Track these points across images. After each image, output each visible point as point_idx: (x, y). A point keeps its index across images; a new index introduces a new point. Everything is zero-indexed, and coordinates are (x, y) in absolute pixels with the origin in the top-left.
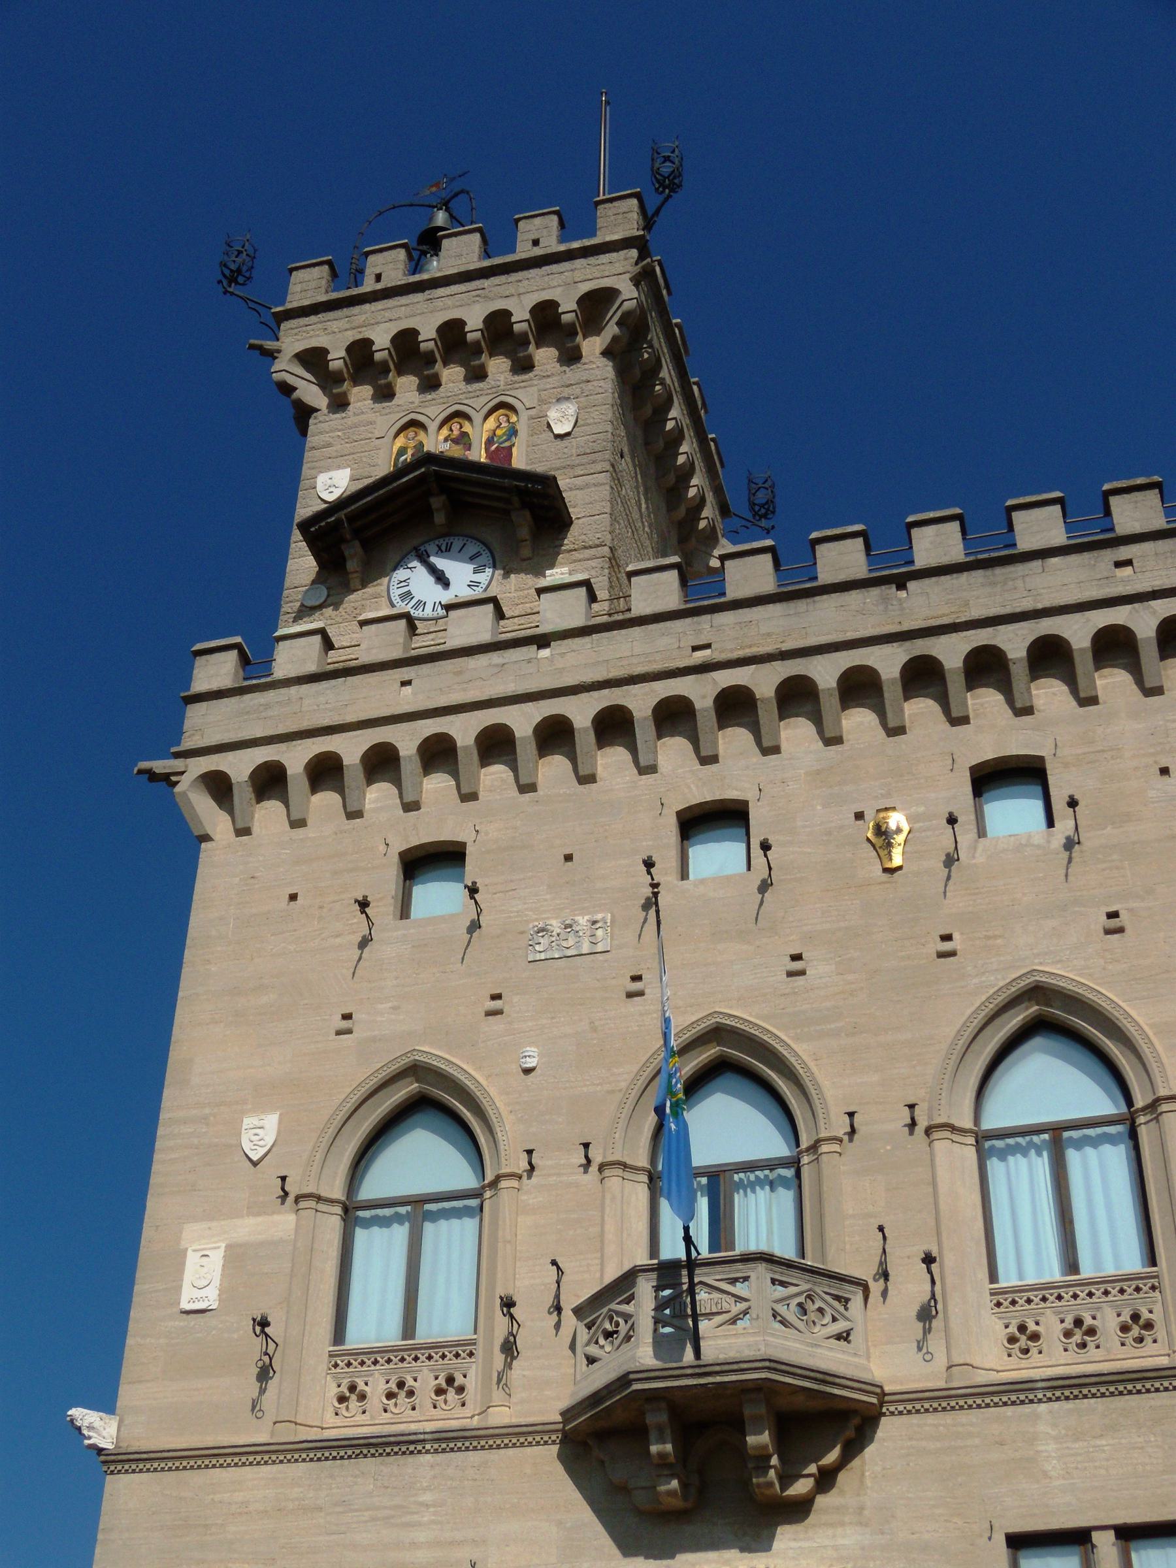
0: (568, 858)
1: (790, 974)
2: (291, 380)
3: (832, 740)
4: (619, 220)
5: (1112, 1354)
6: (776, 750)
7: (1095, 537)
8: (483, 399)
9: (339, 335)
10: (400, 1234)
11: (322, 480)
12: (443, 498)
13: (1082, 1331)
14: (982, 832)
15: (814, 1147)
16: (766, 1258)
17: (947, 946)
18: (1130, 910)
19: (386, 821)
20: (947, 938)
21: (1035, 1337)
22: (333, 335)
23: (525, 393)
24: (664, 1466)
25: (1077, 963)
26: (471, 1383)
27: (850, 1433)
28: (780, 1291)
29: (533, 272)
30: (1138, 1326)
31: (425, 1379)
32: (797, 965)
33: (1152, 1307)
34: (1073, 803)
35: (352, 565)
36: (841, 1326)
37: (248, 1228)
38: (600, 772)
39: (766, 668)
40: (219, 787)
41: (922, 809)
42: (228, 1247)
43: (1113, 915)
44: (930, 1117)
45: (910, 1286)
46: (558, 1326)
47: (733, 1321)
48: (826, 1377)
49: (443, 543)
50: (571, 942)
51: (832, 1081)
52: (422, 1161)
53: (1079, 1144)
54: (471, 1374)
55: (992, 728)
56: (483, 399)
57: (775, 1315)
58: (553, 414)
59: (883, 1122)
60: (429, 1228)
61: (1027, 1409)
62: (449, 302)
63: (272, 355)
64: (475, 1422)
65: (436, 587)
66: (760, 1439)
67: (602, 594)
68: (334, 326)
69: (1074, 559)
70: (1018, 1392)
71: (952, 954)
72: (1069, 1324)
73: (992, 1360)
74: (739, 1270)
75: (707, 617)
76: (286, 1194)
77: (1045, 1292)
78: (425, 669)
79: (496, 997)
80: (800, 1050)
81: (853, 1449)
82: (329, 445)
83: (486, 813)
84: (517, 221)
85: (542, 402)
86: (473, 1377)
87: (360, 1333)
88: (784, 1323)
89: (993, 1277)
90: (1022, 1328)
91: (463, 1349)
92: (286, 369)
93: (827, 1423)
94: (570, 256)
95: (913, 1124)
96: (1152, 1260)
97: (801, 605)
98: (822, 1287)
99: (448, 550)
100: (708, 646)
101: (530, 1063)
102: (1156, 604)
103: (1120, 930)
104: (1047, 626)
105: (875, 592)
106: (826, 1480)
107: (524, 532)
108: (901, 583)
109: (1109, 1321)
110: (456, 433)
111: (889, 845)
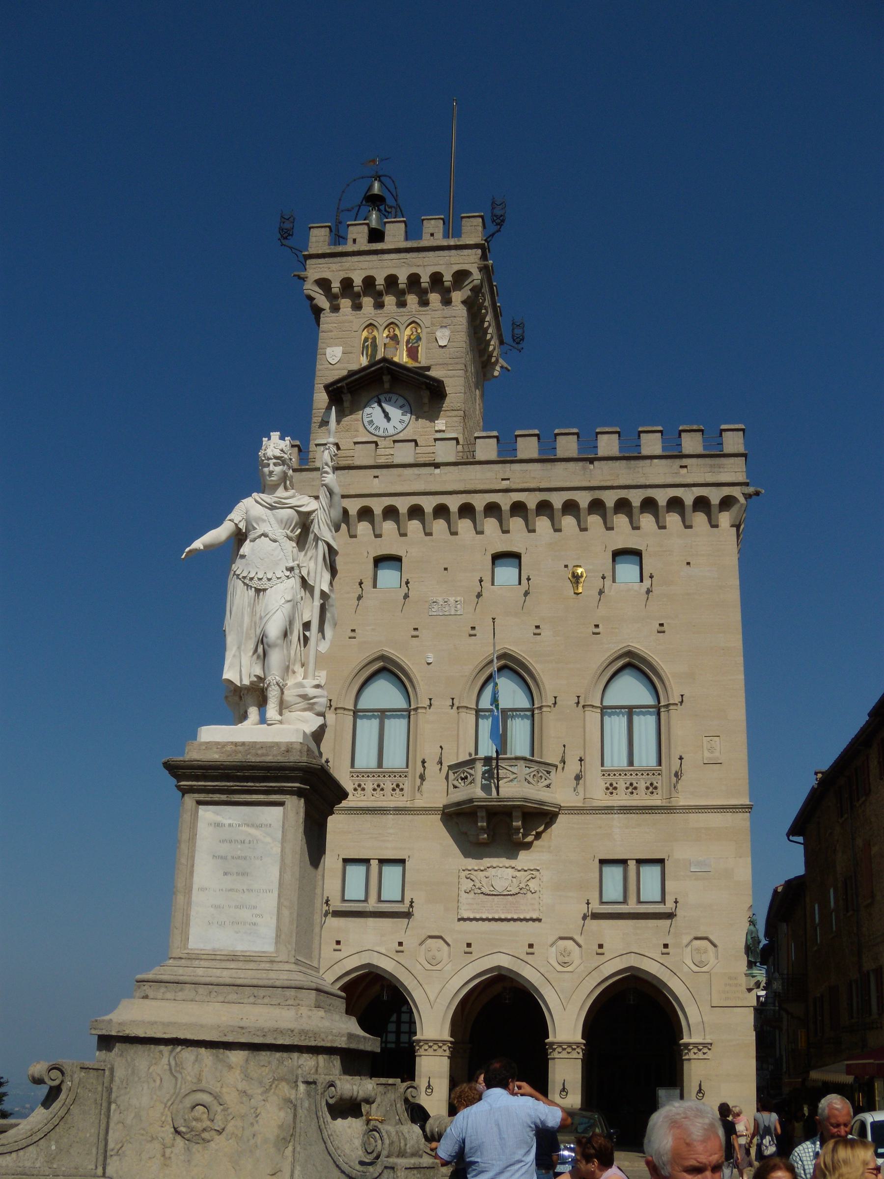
0: (446, 569)
1: (535, 634)
2: (313, 294)
3: (557, 530)
4: (473, 231)
5: (642, 799)
6: (534, 531)
7: (674, 454)
8: (406, 318)
9: (336, 273)
10: (375, 723)
11: (329, 351)
12: (389, 377)
13: (632, 788)
14: (614, 581)
15: (540, 708)
16: (524, 759)
17: (596, 630)
18: (668, 624)
20: (597, 626)
21: (615, 788)
22: (334, 272)
23: (426, 317)
24: (482, 828)
25: (646, 645)
26: (405, 787)
27: (548, 820)
28: (528, 770)
29: (431, 254)
31: (388, 785)
32: (538, 631)
33: (658, 781)
34: (651, 577)
35: (346, 404)
36: (547, 782)
38: (460, 530)
41: (591, 567)
43: (661, 625)
44: (585, 701)
45: (573, 767)
46: (440, 770)
47: (511, 781)
48: (542, 803)
49: (388, 396)
50: (447, 609)
51: (550, 682)
52: (384, 694)
53: (638, 714)
54: (406, 784)
56: (406, 318)
57: (526, 779)
58: (439, 334)
60: (387, 721)
62: (390, 263)
63: (303, 279)
64: (408, 804)
65: (385, 419)
66: (517, 824)
67: (461, 442)
68: (334, 267)
69: (664, 461)
70: (608, 810)
71: (599, 634)
72: (628, 785)
73: (600, 797)
74: (514, 762)
75: (508, 465)
76: (331, 706)
77: (621, 772)
78: (385, 471)
80: (537, 667)
81: (548, 825)
82: (331, 331)
83: (412, 542)
84: (423, 220)
85: (433, 324)
86: (407, 785)
87: (360, 763)
88: (529, 782)
89: (602, 765)
90: (611, 785)
91: (403, 774)
92: (310, 288)
93: (540, 817)
94: (449, 248)
95: (578, 703)
96: (660, 763)
97: (548, 465)
98: (542, 768)
99: (390, 400)
100: (508, 479)
101: (430, 661)
103: (664, 632)
104: (650, 493)
105: (580, 464)
106: (538, 836)
107: (426, 400)
108: (591, 461)
109: (642, 785)
110: (392, 333)
111: (577, 583)
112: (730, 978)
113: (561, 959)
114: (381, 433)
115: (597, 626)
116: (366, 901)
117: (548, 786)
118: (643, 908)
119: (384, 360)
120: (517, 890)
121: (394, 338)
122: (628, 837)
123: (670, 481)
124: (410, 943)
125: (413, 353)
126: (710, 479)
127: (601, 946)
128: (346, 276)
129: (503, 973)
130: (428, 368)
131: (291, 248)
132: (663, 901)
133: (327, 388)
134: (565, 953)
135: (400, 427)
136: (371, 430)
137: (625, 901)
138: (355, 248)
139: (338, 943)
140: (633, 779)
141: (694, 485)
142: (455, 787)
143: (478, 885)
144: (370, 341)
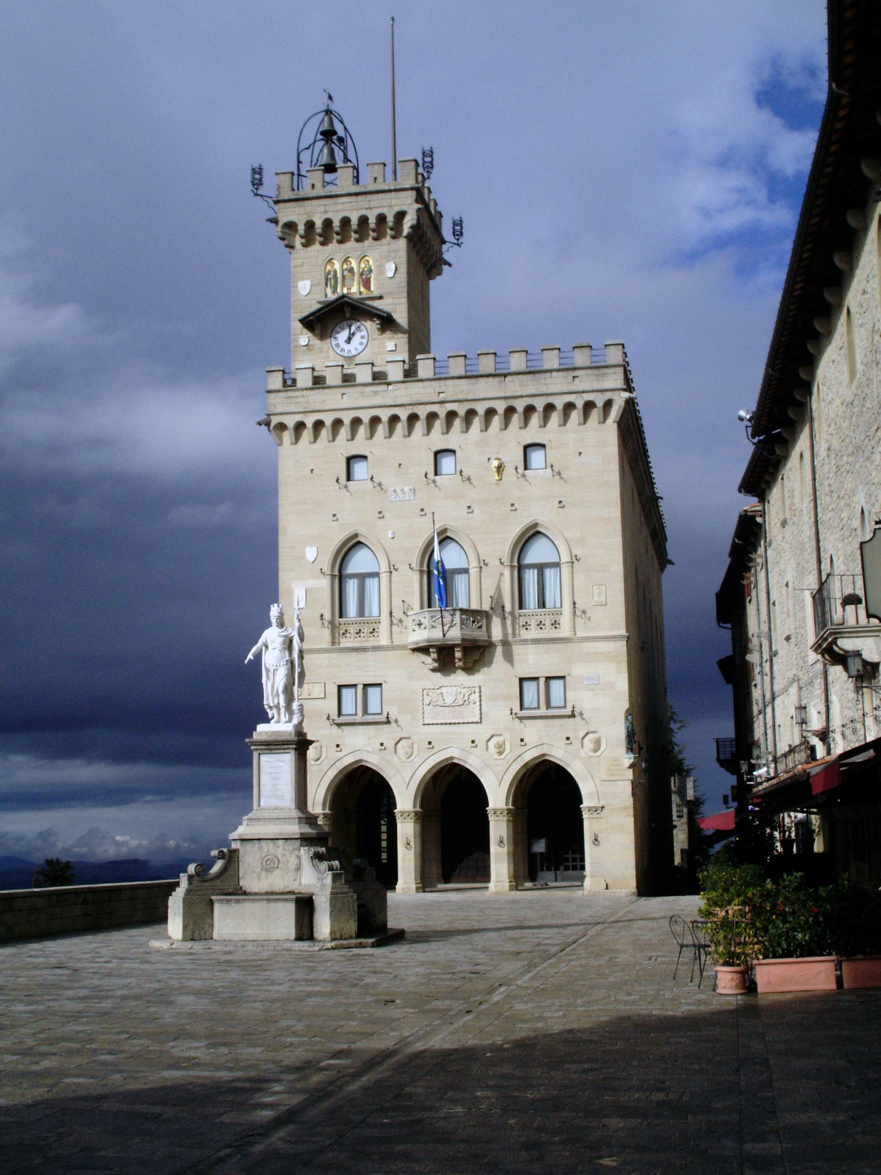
5: (548, 633)
13: (540, 624)
29: (375, 196)
30: (555, 624)
31: (366, 629)
34: (552, 466)
36: (480, 624)
37: (311, 583)
39: (461, 405)
43: (560, 502)
48: (475, 641)
49: (349, 322)
61: (526, 646)
69: (560, 374)
79: (380, 512)
85: (381, 258)
97: (473, 380)
102: (584, 395)
105: (497, 379)
109: (548, 623)
112: (614, 760)
114: (346, 354)
115: (512, 505)
116: (356, 714)
117: (480, 627)
118: (550, 712)
119: (343, 296)
120: (461, 702)
121: (351, 270)
123: (565, 389)
124: (389, 744)
125: (367, 284)
126: (596, 387)
127: (522, 740)
128: (309, 219)
129: (455, 761)
130: (381, 298)
131: (261, 196)
132: (565, 707)
133: (302, 321)
135: (360, 348)
136: (338, 351)
137: (538, 708)
138: (314, 193)
139: (338, 746)
140: (542, 618)
144: (332, 274)
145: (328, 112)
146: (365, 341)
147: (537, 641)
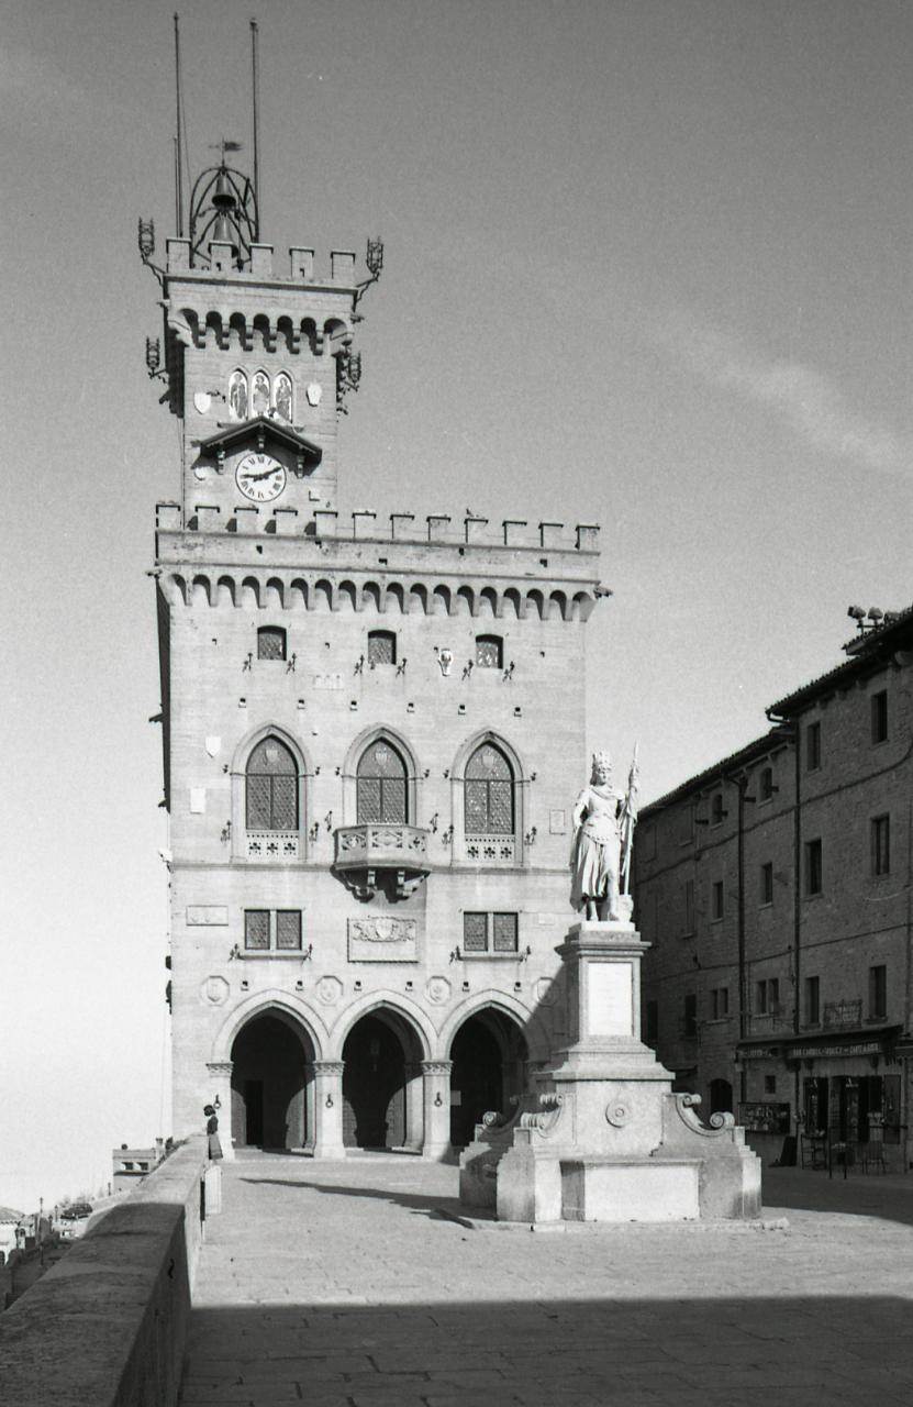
8: (276, 367)
15: (415, 779)
19: (252, 612)
34: (512, 666)
40: (179, 580)
42: (207, 790)
55: (486, 622)
59: (437, 774)
103: (520, 716)
109: (498, 851)
110: (260, 384)
113: (434, 995)
122: (490, 895)
130: (301, 430)
134: (438, 990)
136: (246, 492)
139: (245, 983)
141: (552, 580)
142: (345, 848)
143: (365, 932)
145: (223, 170)
146: (281, 483)
147: (486, 871)
